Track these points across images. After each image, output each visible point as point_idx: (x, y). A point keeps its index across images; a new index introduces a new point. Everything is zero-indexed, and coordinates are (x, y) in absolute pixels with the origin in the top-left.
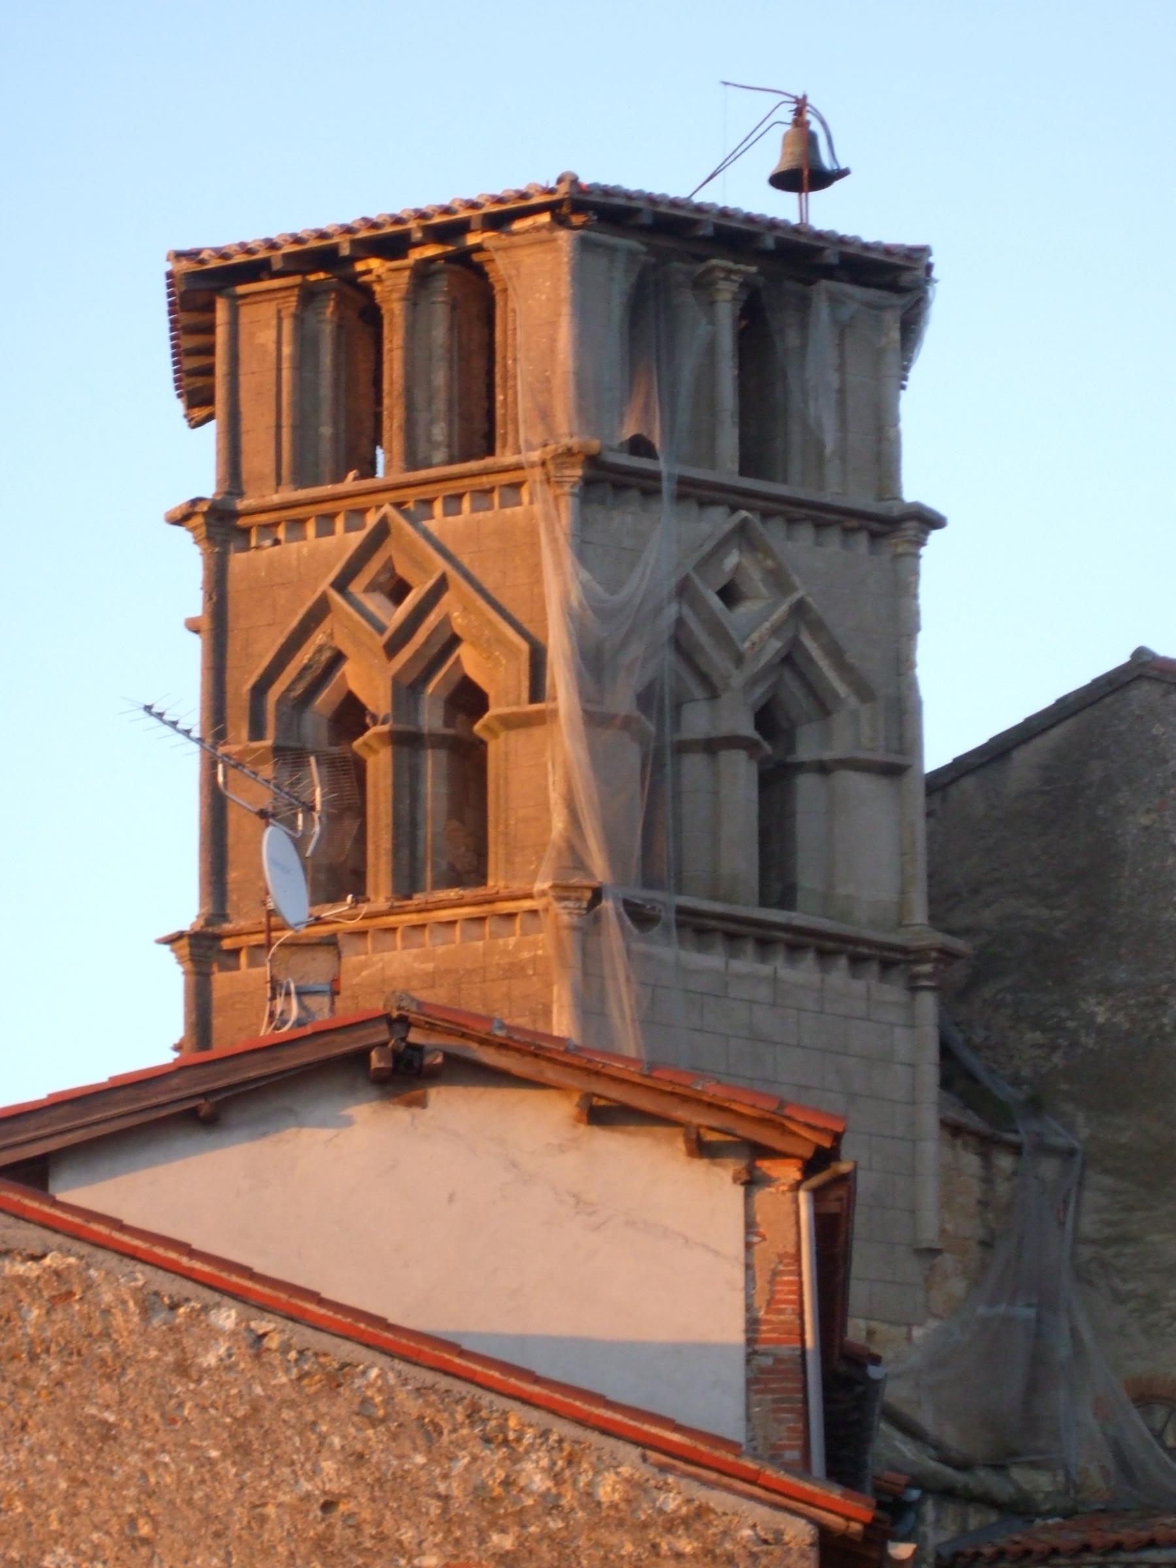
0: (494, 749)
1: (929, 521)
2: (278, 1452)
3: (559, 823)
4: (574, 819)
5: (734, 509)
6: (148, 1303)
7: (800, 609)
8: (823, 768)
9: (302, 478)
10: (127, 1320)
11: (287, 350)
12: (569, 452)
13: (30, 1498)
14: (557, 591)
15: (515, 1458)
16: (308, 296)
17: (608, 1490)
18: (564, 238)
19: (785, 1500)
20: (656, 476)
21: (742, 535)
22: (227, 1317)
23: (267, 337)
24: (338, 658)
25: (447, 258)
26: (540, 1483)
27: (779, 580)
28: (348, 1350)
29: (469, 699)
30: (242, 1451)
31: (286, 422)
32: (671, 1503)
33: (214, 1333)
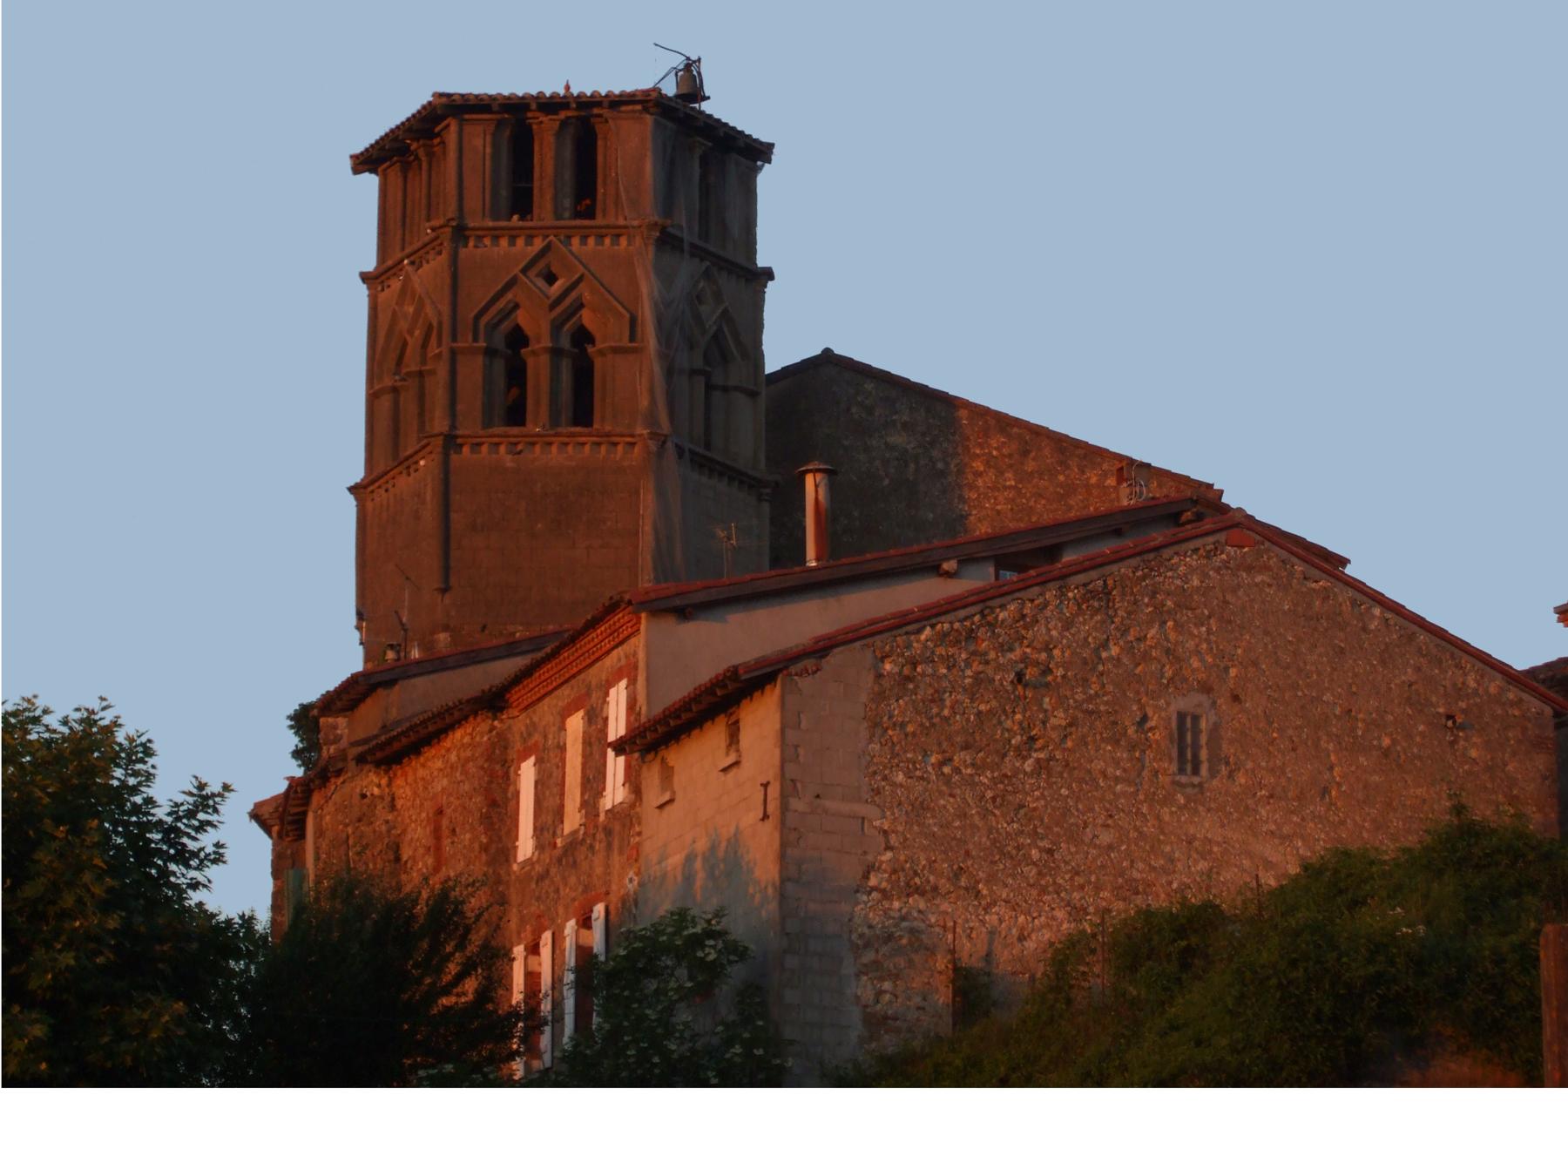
0: (598, 363)
1: (768, 274)
2: (906, 671)
3: (644, 402)
4: (653, 401)
5: (702, 260)
6: (1354, 602)
7: (725, 312)
8: (725, 389)
9: (496, 216)
10: (1347, 607)
11: (488, 150)
12: (656, 224)
13: (1319, 674)
14: (648, 289)
15: (1465, 674)
16: (499, 123)
17: (1493, 690)
18: (649, 119)
19: (1545, 699)
20: (681, 240)
21: (707, 274)
22: (1377, 611)
23: (478, 142)
24: (517, 306)
25: (577, 118)
26: (1473, 684)
27: (718, 296)
28: (1415, 628)
29: (583, 337)
30: (1383, 662)
31: (488, 185)
32: (1511, 696)
33: (1373, 617)
